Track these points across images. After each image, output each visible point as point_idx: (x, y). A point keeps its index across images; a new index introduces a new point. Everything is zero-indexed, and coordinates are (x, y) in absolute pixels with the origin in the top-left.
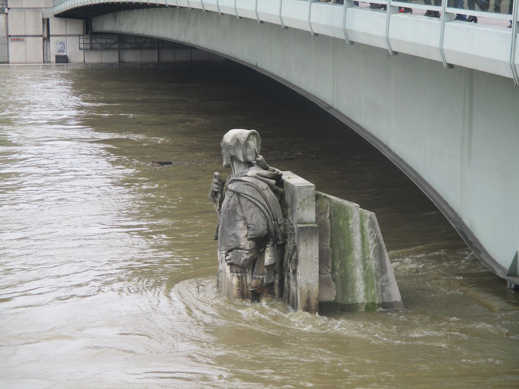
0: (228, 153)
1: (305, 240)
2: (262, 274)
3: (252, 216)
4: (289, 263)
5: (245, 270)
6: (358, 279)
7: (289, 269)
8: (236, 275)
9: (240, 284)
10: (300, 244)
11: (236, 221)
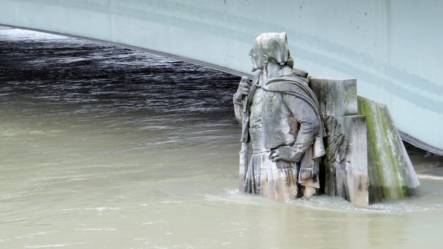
1: (356, 129)
2: (310, 166)
3: (304, 111)
4: (337, 154)
5: (290, 165)
6: (384, 166)
7: (335, 159)
8: (283, 170)
9: (287, 178)
10: (352, 133)
11: (280, 119)
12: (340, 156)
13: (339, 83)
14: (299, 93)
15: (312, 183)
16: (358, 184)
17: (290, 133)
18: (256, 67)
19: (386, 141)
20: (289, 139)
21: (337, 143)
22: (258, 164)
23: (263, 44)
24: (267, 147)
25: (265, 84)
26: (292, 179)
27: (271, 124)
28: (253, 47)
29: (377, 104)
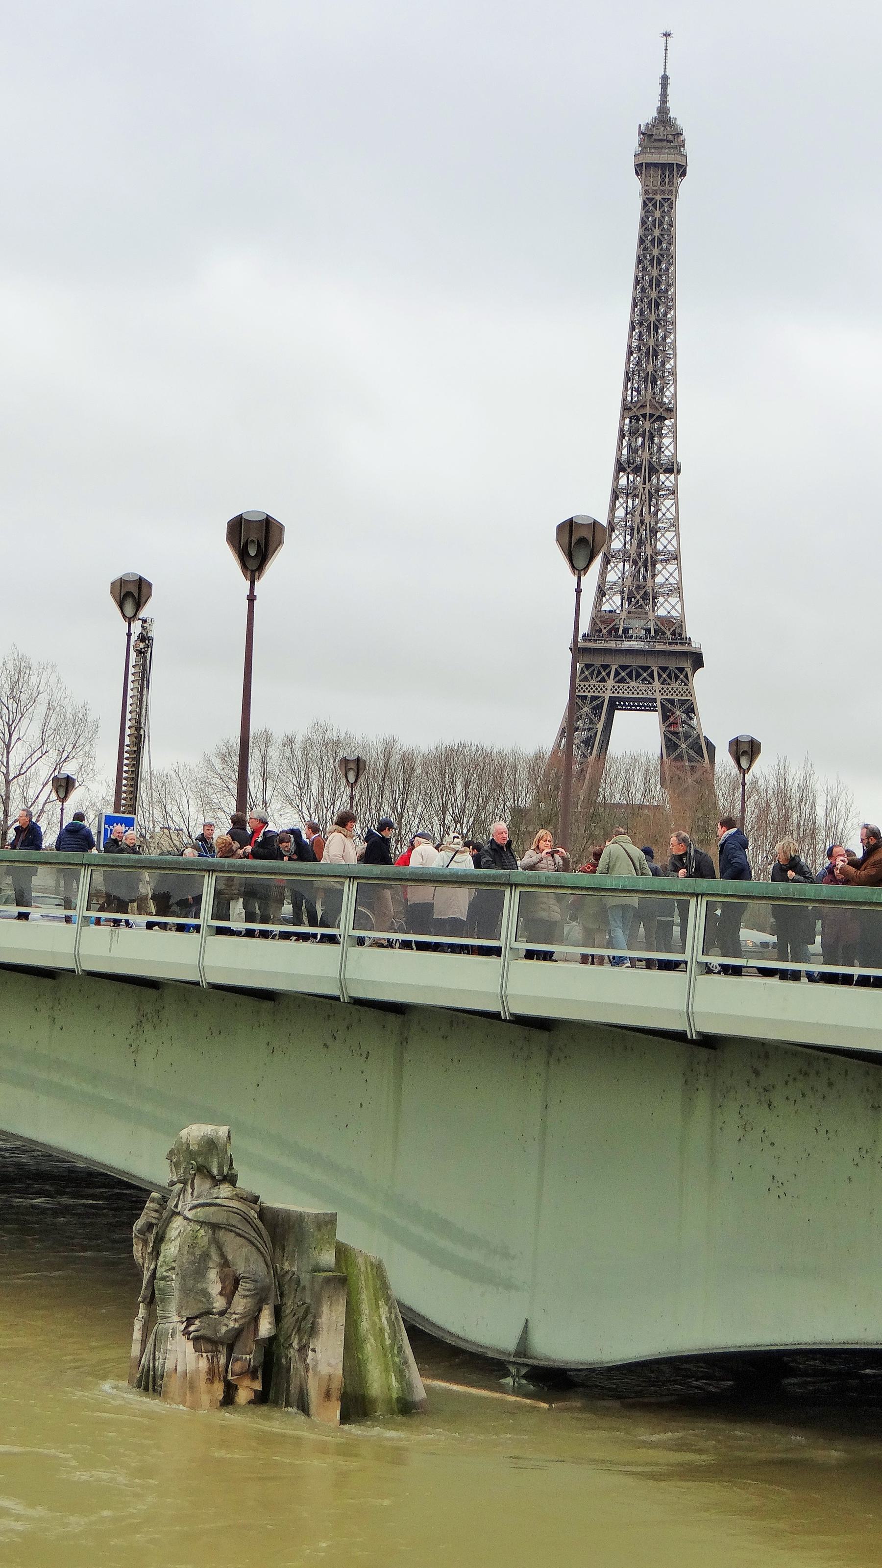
0: (192, 1162)
3: (247, 1260)
5: (216, 1349)
6: (370, 1360)
8: (204, 1355)
9: (209, 1370)
10: (323, 1303)
11: (207, 1268)
12: (300, 1341)
13: (309, 1218)
14: (243, 1229)
15: (249, 1380)
16: (324, 1390)
17: (221, 1294)
18: (175, 1179)
19: (377, 1320)
20: (219, 1303)
21: (297, 1316)
22: (163, 1341)
23: (191, 1142)
24: (181, 1314)
25: (187, 1209)
26: (216, 1371)
27: (191, 1276)
28: (173, 1147)
29: (366, 1256)
